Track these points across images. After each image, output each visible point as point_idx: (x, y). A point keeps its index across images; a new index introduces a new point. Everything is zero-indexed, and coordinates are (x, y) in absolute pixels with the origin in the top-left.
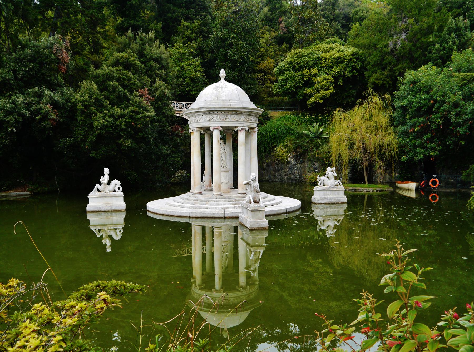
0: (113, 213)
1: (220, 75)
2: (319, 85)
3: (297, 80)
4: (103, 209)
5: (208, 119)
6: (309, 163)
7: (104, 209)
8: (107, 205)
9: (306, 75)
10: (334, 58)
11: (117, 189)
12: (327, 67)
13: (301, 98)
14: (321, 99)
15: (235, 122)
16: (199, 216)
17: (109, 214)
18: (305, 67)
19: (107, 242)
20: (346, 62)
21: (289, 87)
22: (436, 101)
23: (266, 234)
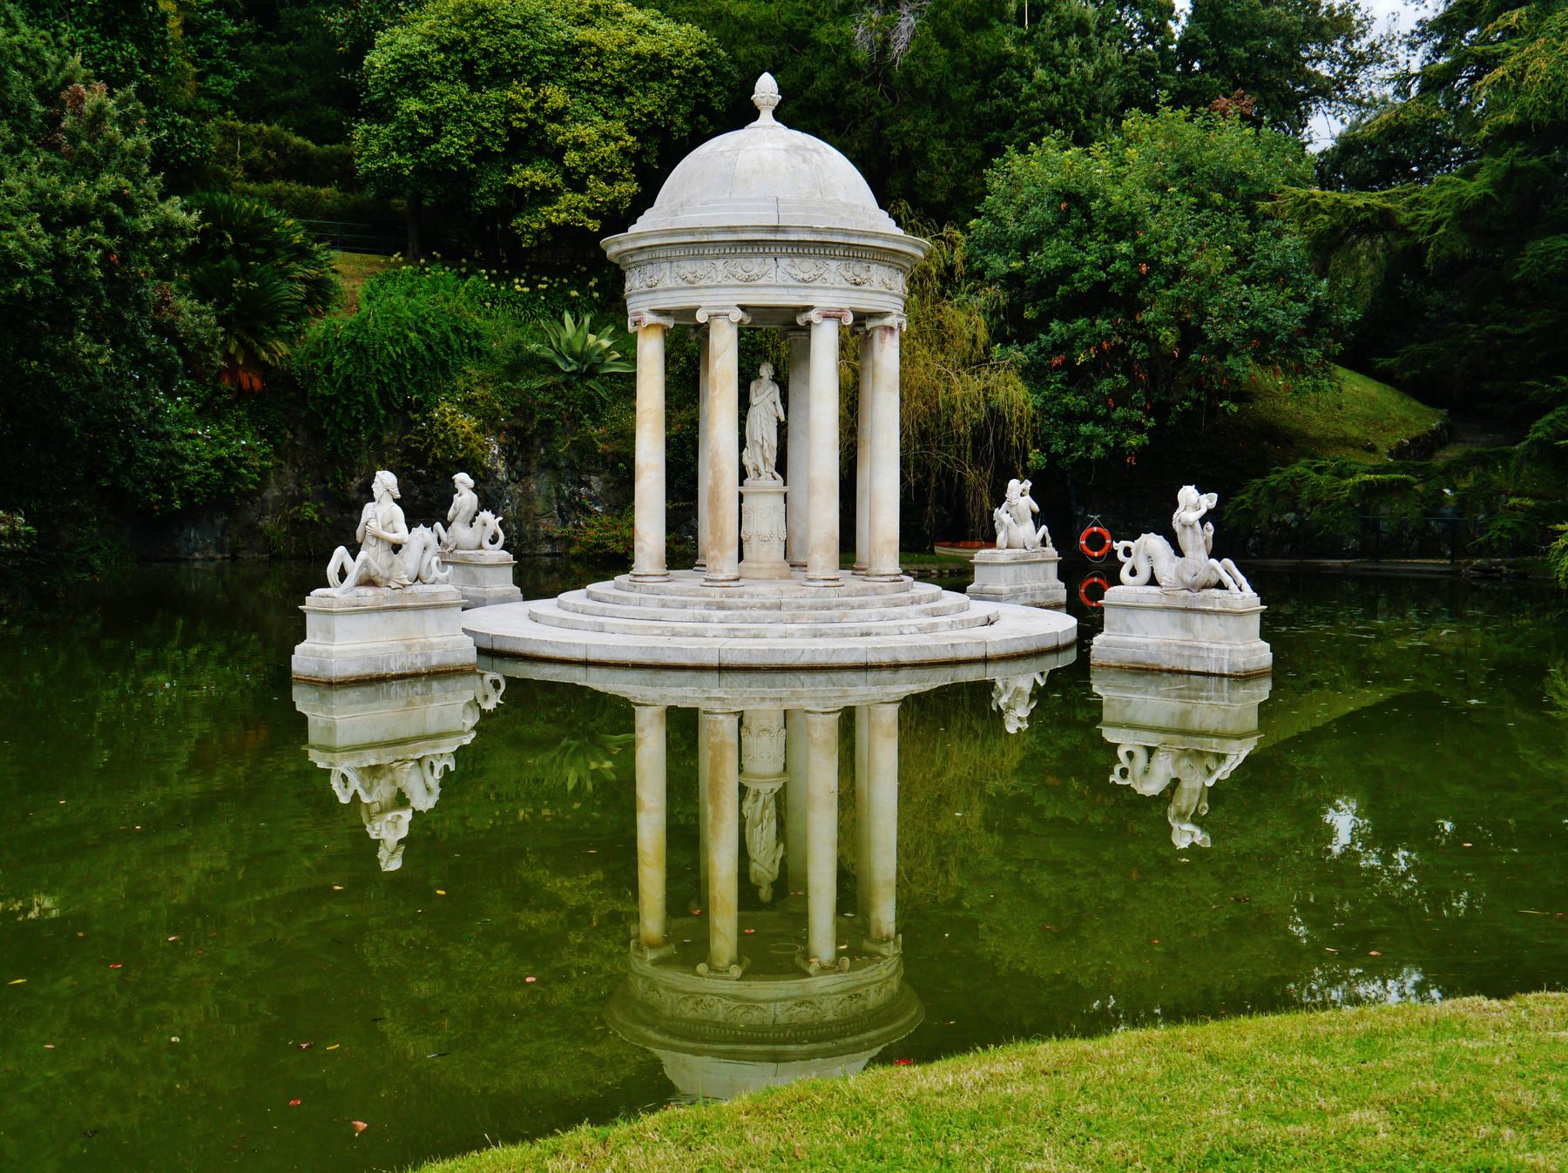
0: (435, 685)
1: (757, 97)
2: (583, 159)
3: (486, 125)
4: (395, 669)
5: (806, 276)
6: (545, 478)
7: (402, 667)
8: (409, 647)
9: (521, 110)
10: (638, 57)
12: (605, 85)
13: (493, 201)
14: (592, 214)
15: (886, 298)
16: (903, 658)
17: (419, 687)
18: (517, 74)
20: (679, 77)
21: (452, 151)
22: (1154, 265)
23: (1264, 690)
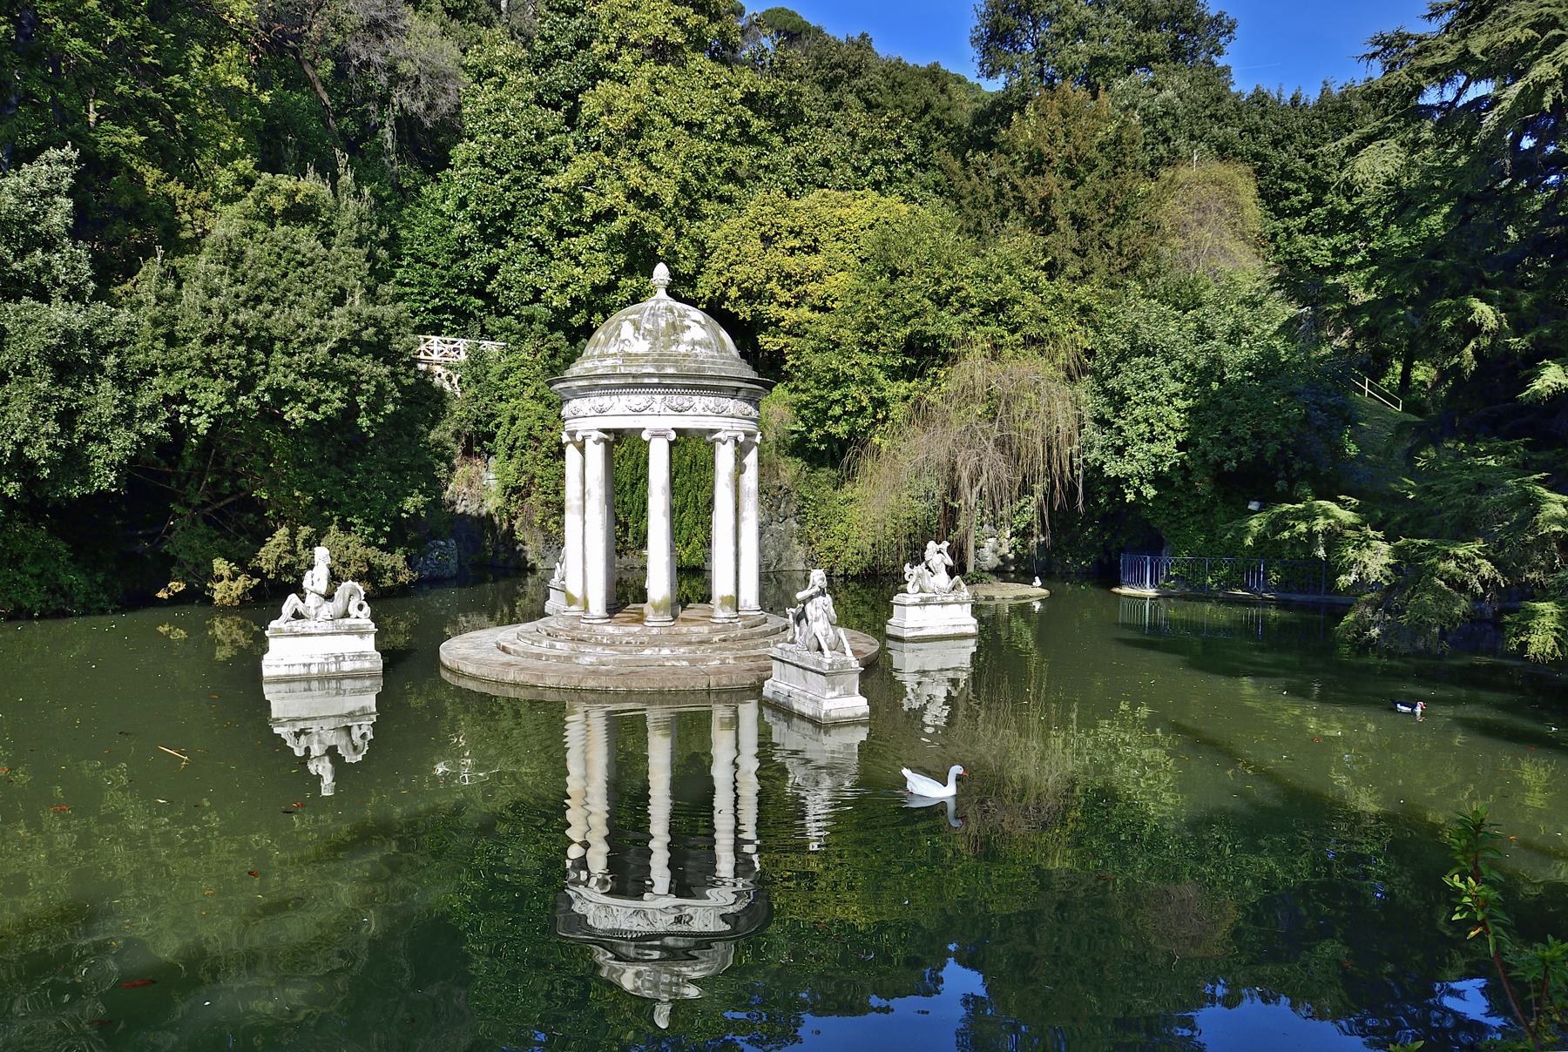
11: (353, 610)
19: (323, 769)
